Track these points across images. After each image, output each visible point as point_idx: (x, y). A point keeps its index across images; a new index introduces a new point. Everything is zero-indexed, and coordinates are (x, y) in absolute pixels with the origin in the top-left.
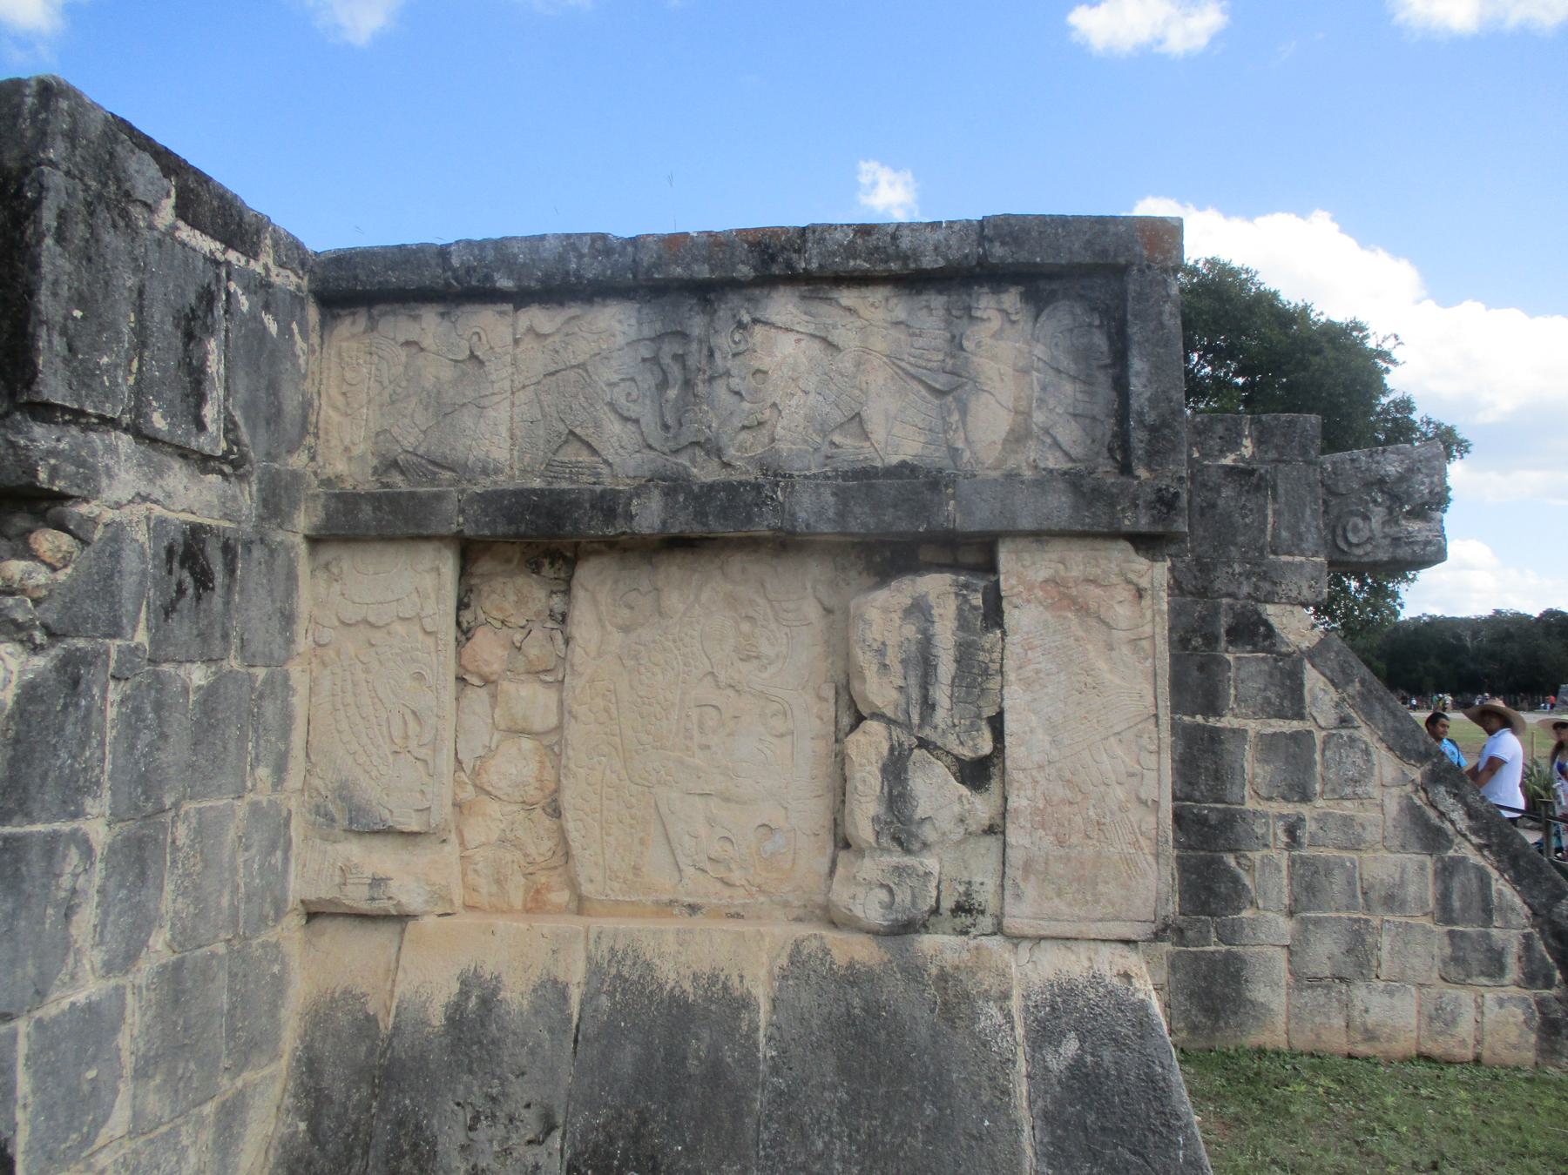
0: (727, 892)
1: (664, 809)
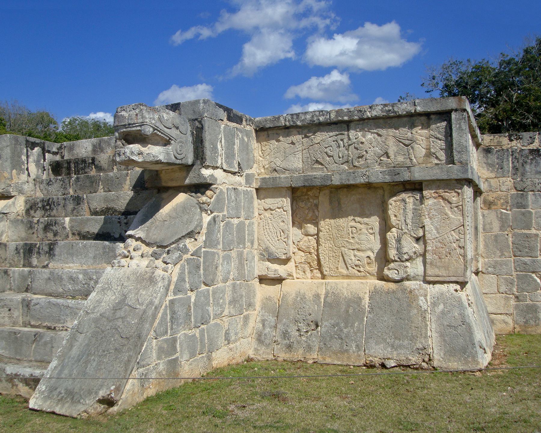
0: (359, 274)
1: (343, 253)
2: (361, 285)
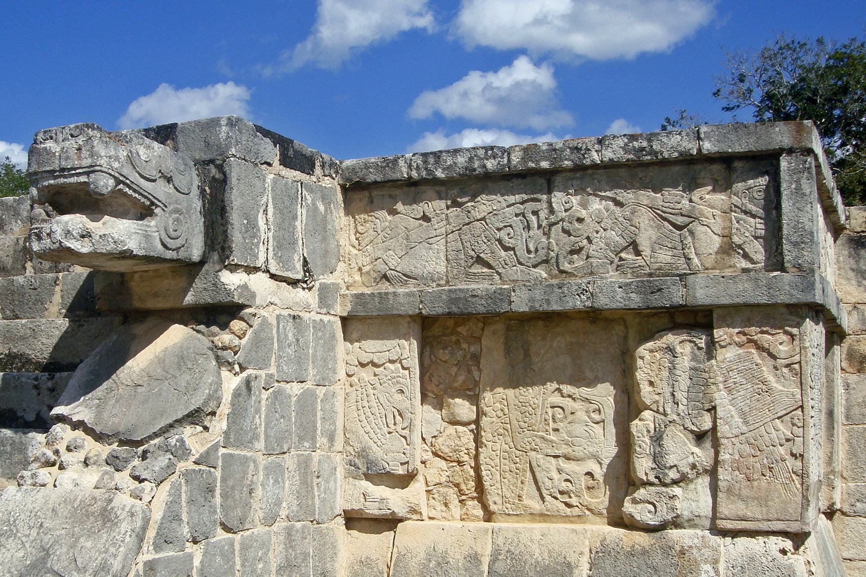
0: (568, 511)
1: (534, 464)
2: (573, 536)
